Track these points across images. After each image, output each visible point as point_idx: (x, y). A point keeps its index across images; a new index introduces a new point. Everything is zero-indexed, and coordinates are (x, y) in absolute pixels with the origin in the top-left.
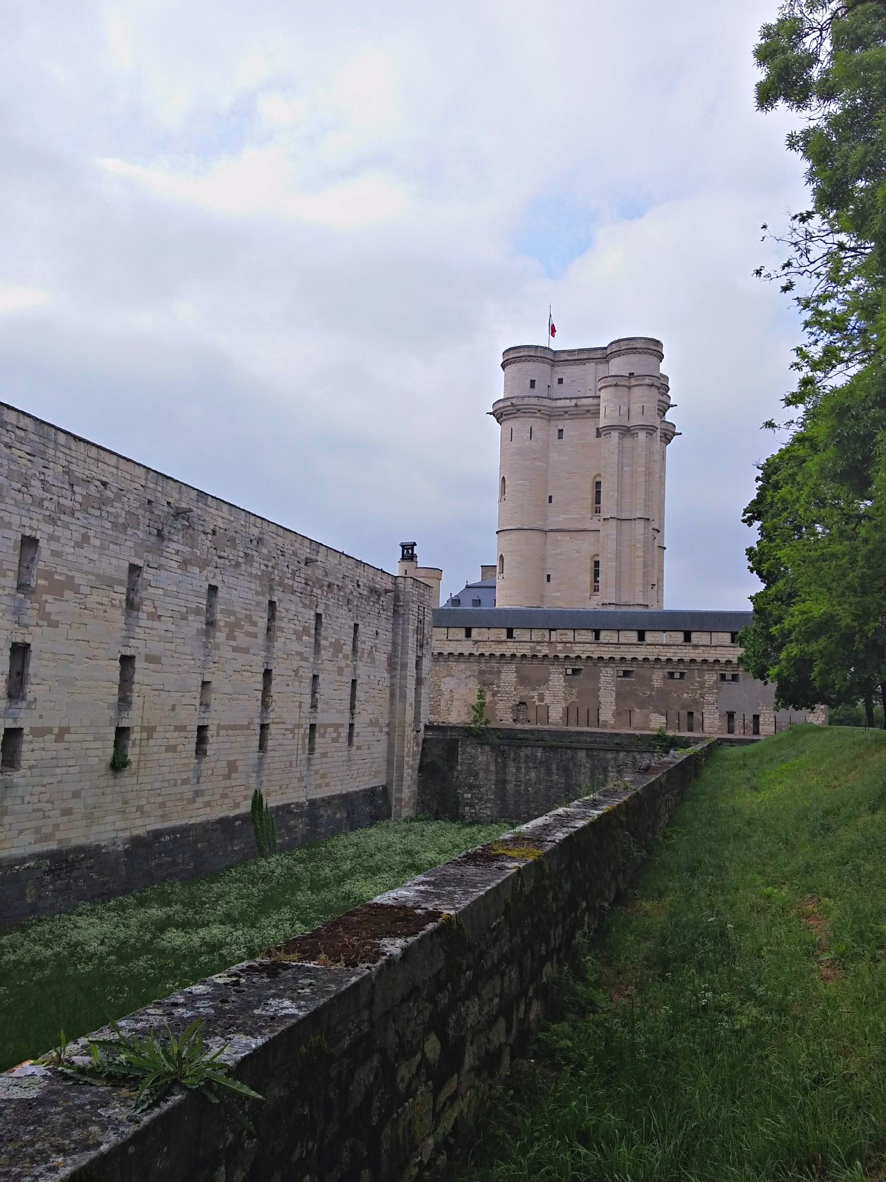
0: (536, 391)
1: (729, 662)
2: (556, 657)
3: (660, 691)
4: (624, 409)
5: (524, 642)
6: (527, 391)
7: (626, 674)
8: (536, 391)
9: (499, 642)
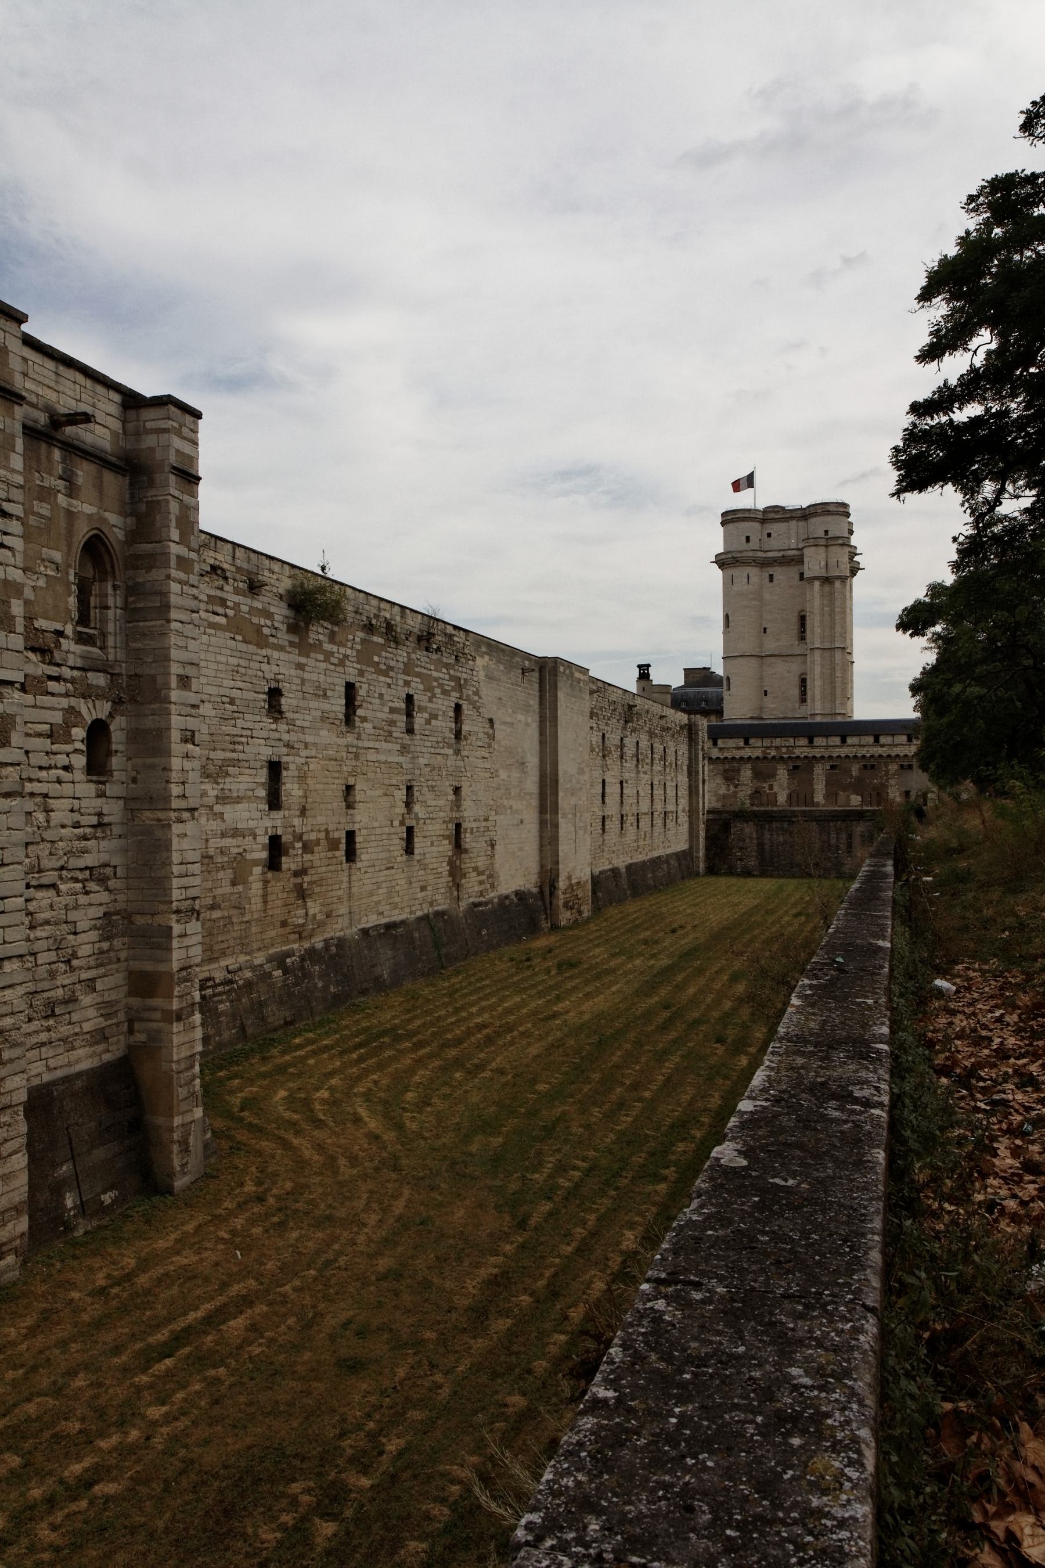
1: (906, 756)
2: (782, 758)
4: (823, 563)
5: (756, 748)
6: (744, 546)
9: (738, 748)
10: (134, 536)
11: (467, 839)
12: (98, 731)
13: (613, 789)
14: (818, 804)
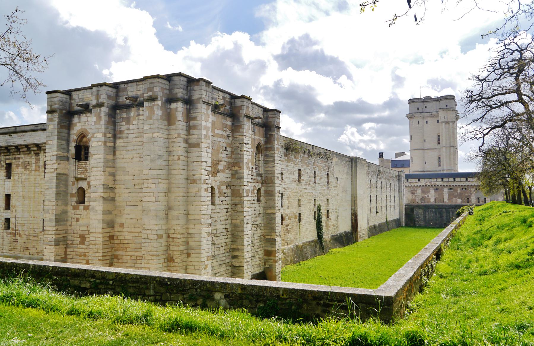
0: (419, 111)
3: (460, 193)
4: (446, 117)
7: (450, 189)
8: (419, 111)
10: (266, 142)
11: (330, 215)
12: (259, 190)
13: (374, 199)
14: (445, 202)
